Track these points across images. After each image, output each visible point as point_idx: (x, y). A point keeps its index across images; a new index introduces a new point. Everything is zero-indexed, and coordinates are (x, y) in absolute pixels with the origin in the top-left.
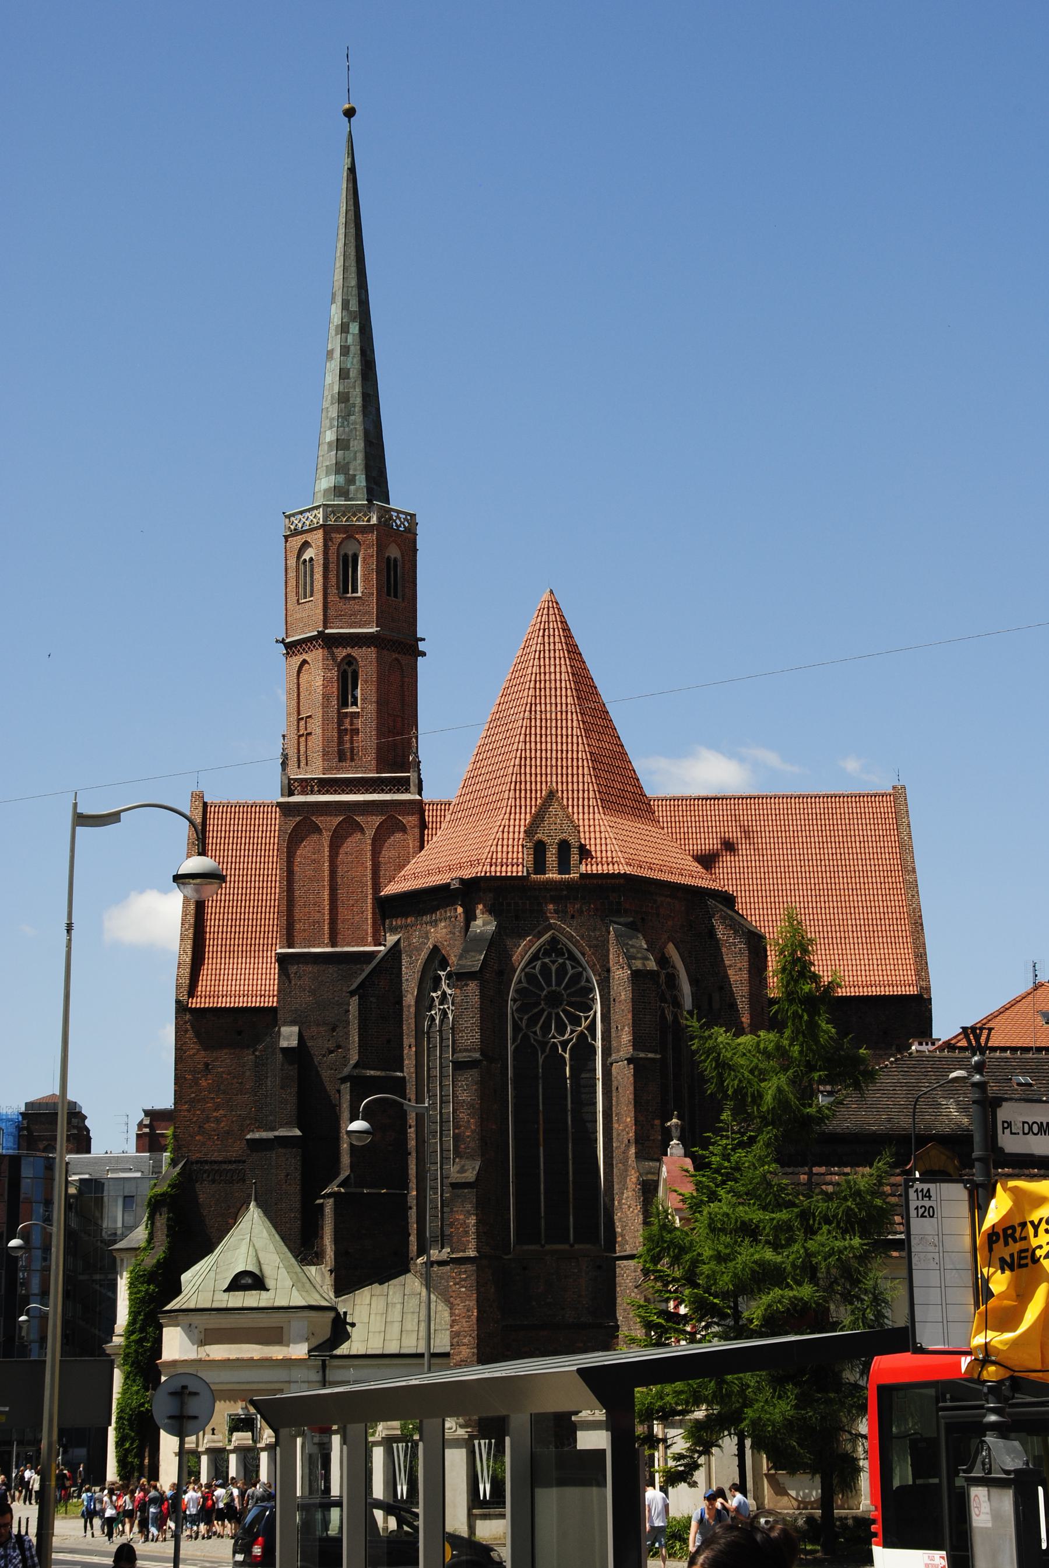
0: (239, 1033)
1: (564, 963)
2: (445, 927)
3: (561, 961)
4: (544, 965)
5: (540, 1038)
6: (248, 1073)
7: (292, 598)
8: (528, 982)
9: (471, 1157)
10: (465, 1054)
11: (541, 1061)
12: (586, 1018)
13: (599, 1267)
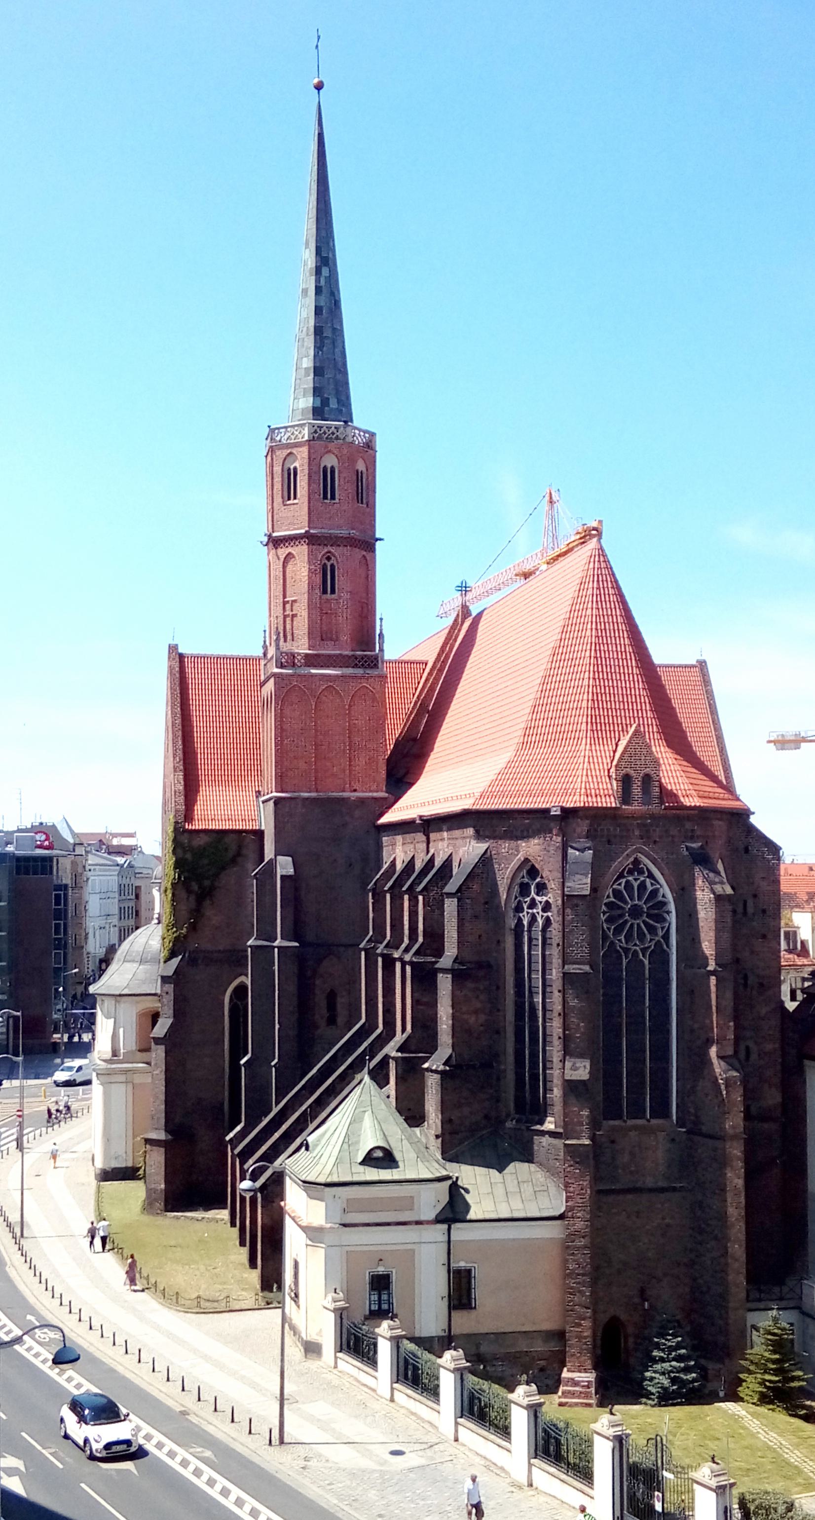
1: (644, 881)
3: (642, 879)
4: (627, 882)
7: (278, 499)
9: (581, 1056)
10: (575, 966)
13: (673, 1140)
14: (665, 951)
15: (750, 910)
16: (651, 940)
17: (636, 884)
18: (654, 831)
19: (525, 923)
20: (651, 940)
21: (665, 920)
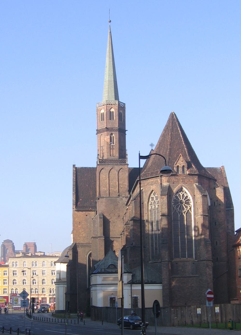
0: (87, 216)
2: (155, 186)
5: (179, 211)
6: (89, 224)
8: (176, 198)
11: (179, 216)
12: (189, 207)
13: (194, 263)
14: (190, 213)
15: (216, 204)
16: (186, 210)
17: (181, 195)
18: (186, 180)
19: (153, 208)
20: (186, 210)
21: (190, 204)
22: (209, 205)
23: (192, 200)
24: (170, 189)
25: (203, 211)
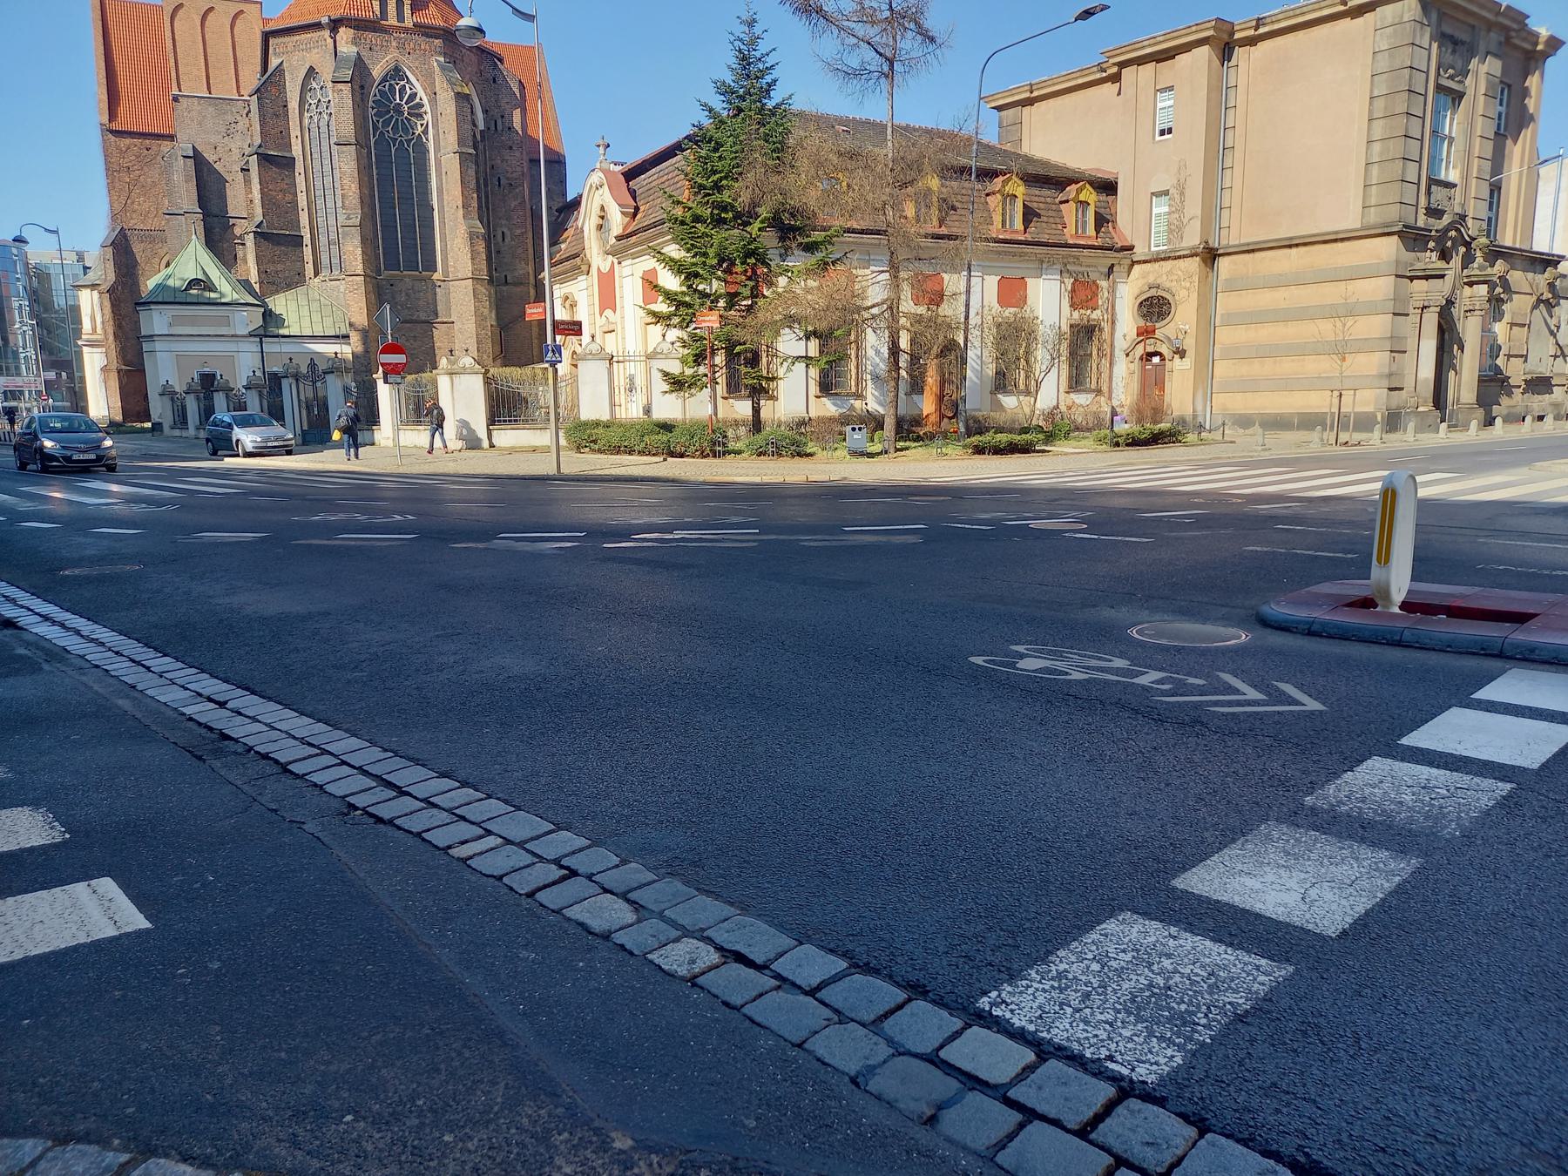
22: (481, 126)
23: (427, 108)
24: (360, 66)
25: (461, 142)
